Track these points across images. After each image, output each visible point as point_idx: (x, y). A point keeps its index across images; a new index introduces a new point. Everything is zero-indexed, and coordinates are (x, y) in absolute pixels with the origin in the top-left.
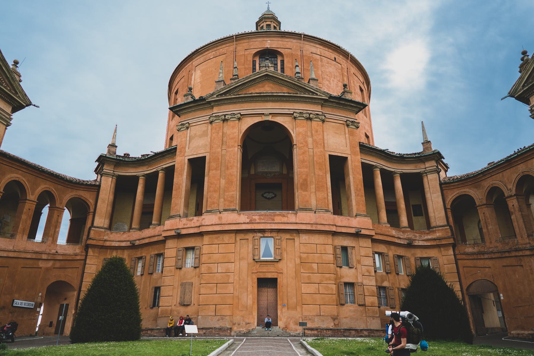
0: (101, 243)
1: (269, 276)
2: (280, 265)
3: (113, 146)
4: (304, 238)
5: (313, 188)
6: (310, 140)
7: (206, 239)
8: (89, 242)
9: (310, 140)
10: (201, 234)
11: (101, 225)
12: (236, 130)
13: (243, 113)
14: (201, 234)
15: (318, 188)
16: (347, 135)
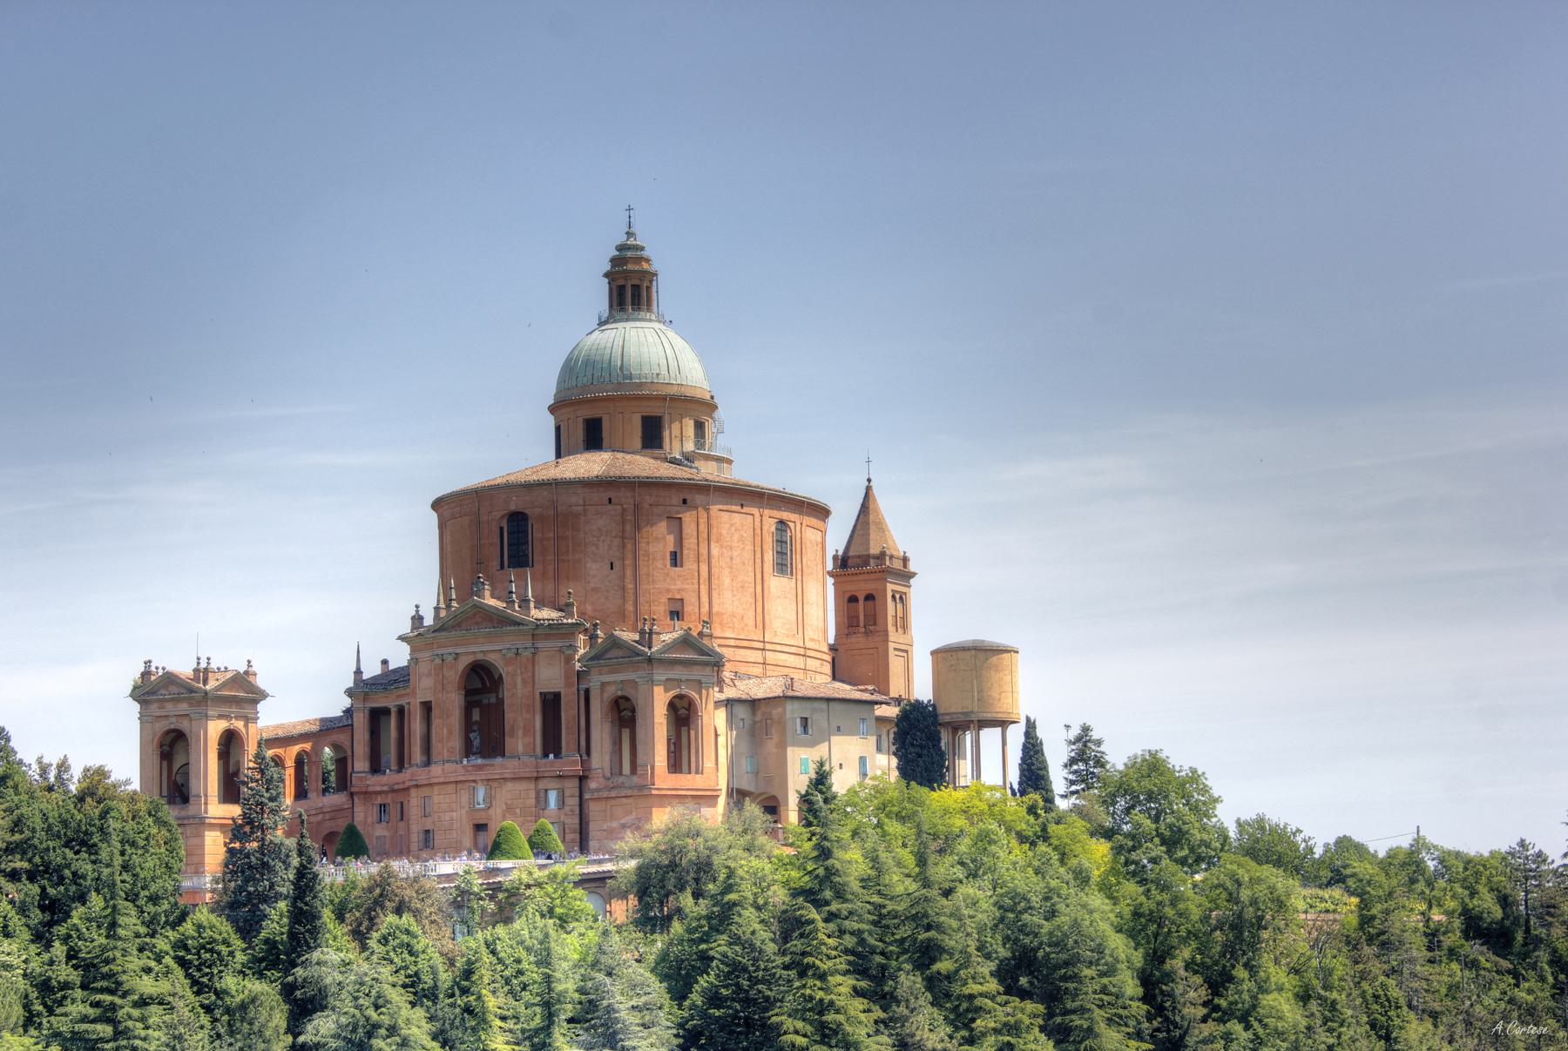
0: (364, 790)
1: (481, 822)
2: (491, 811)
3: (358, 672)
4: (510, 785)
5: (520, 733)
6: (519, 679)
7: (436, 788)
8: (353, 790)
9: (519, 679)
10: (431, 785)
11: (362, 769)
12: (452, 673)
13: (458, 651)
14: (431, 785)
15: (525, 735)
16: (562, 664)
